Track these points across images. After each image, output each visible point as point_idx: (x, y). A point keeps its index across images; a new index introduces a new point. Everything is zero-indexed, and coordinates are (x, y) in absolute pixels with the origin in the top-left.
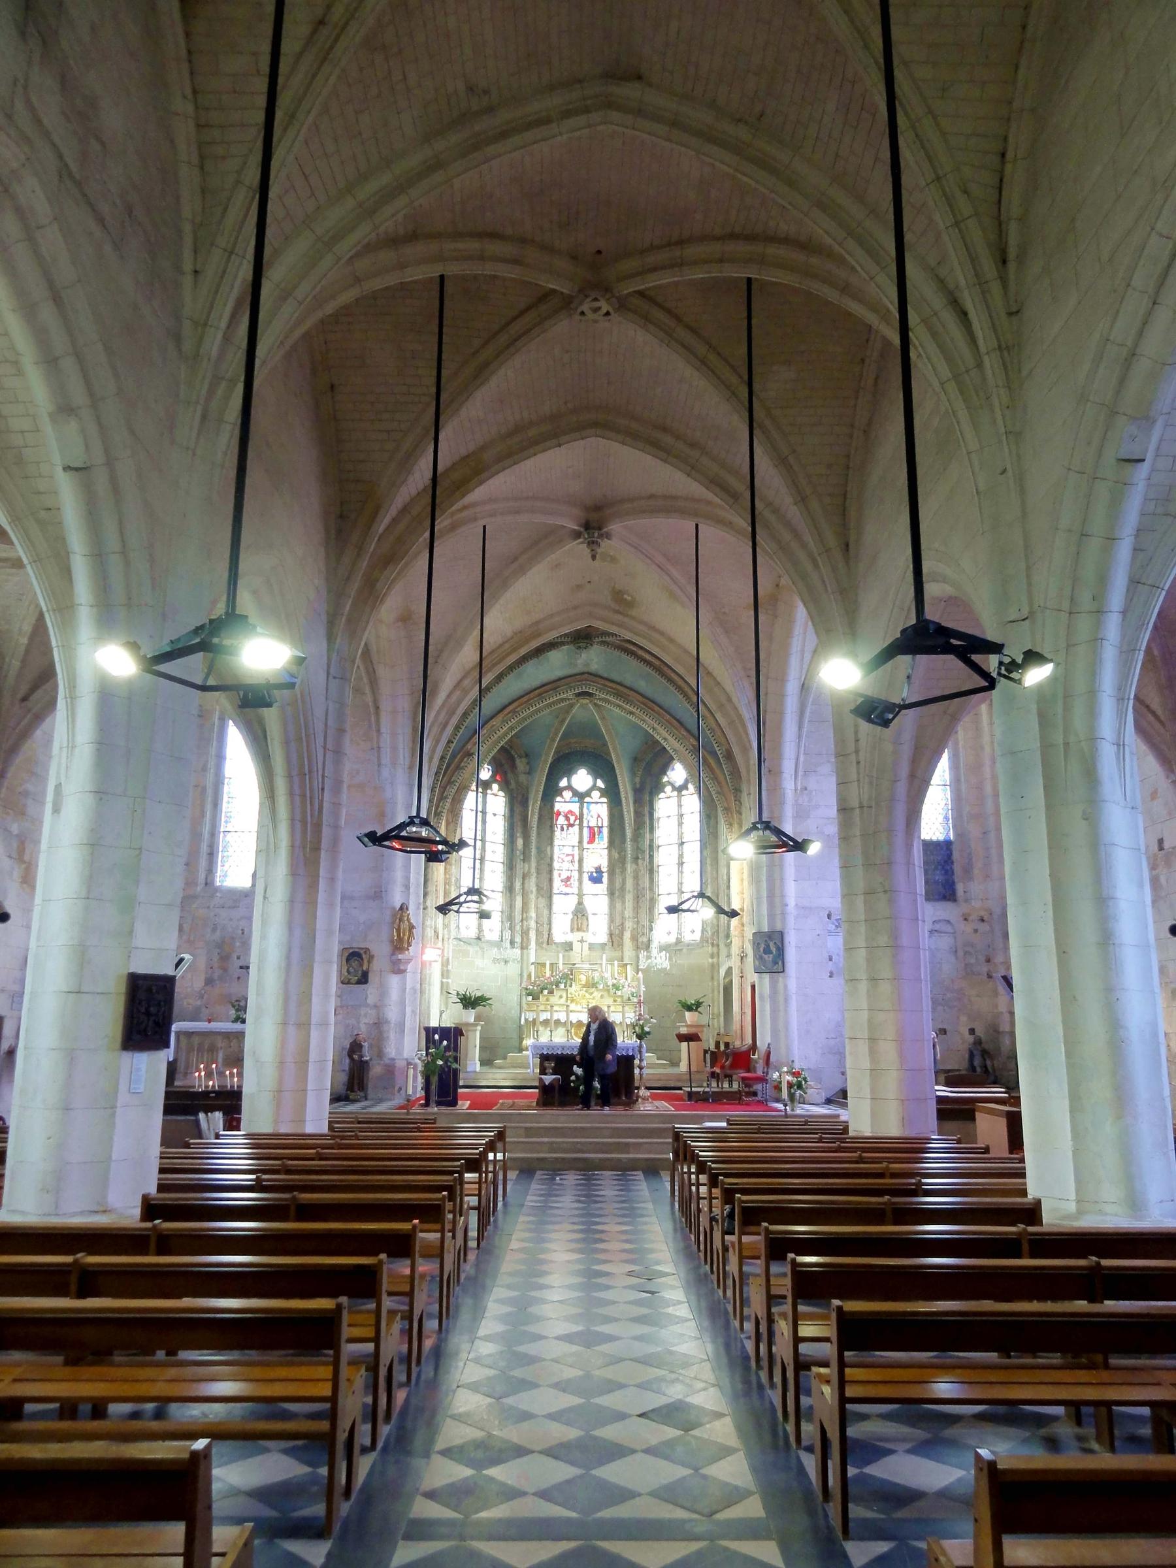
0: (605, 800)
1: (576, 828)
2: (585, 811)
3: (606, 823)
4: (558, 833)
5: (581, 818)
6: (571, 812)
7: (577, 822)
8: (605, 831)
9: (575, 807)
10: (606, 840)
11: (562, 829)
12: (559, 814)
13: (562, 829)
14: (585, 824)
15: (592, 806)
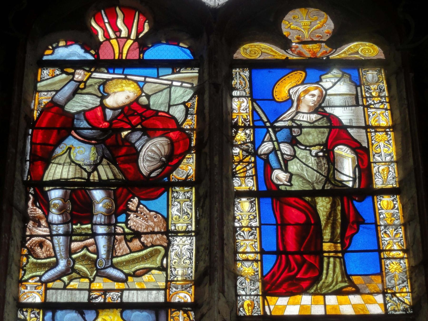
0: (365, 49)
1: (182, 209)
2: (241, 107)
3: (385, 174)
4: (47, 228)
5: (213, 133)
6: (139, 116)
7: (188, 167)
8: (388, 208)
9: (174, 93)
10: (397, 267)
11: (79, 208)
12: (61, 123)
13: (79, 208)
14: (244, 183)
15: (287, 87)
